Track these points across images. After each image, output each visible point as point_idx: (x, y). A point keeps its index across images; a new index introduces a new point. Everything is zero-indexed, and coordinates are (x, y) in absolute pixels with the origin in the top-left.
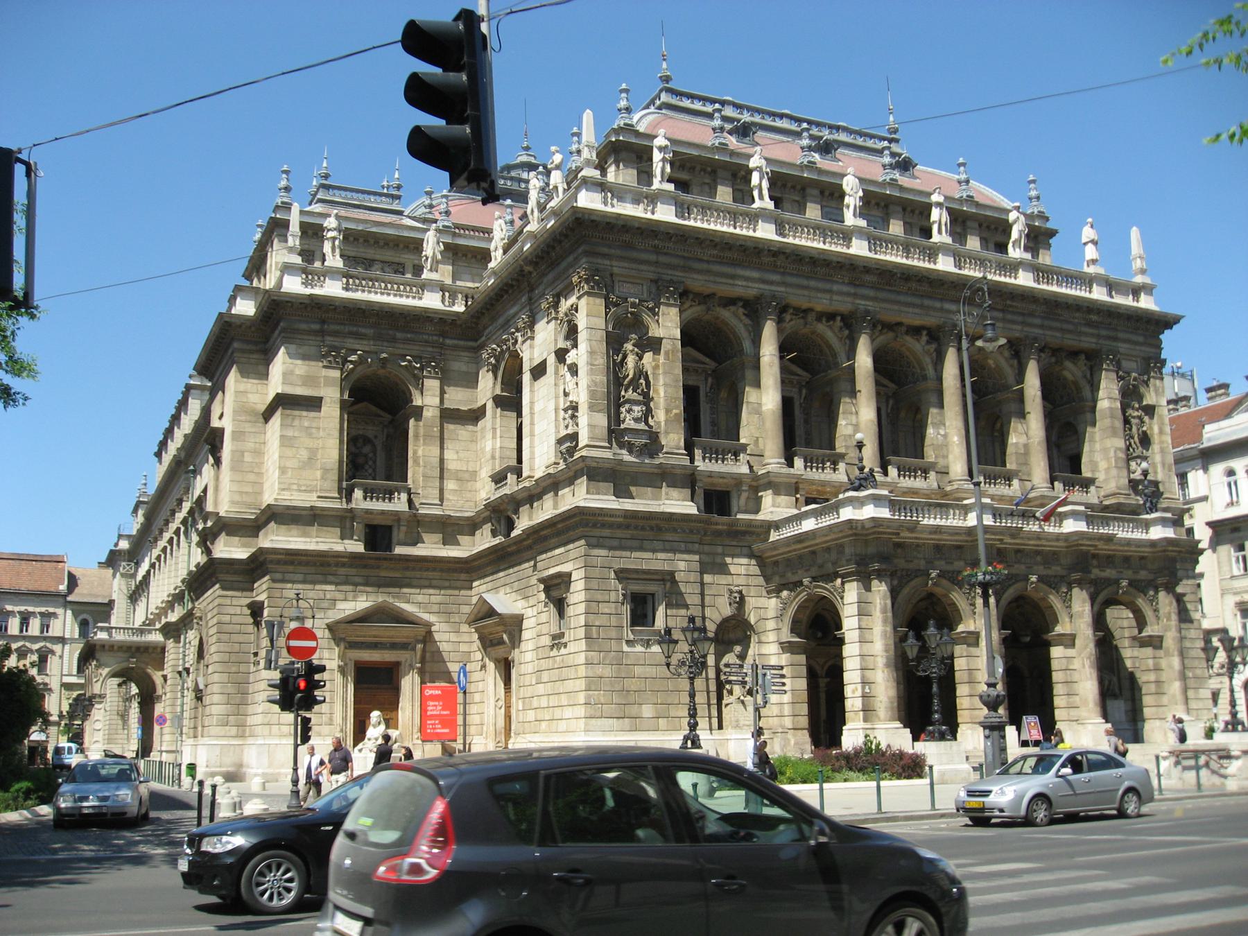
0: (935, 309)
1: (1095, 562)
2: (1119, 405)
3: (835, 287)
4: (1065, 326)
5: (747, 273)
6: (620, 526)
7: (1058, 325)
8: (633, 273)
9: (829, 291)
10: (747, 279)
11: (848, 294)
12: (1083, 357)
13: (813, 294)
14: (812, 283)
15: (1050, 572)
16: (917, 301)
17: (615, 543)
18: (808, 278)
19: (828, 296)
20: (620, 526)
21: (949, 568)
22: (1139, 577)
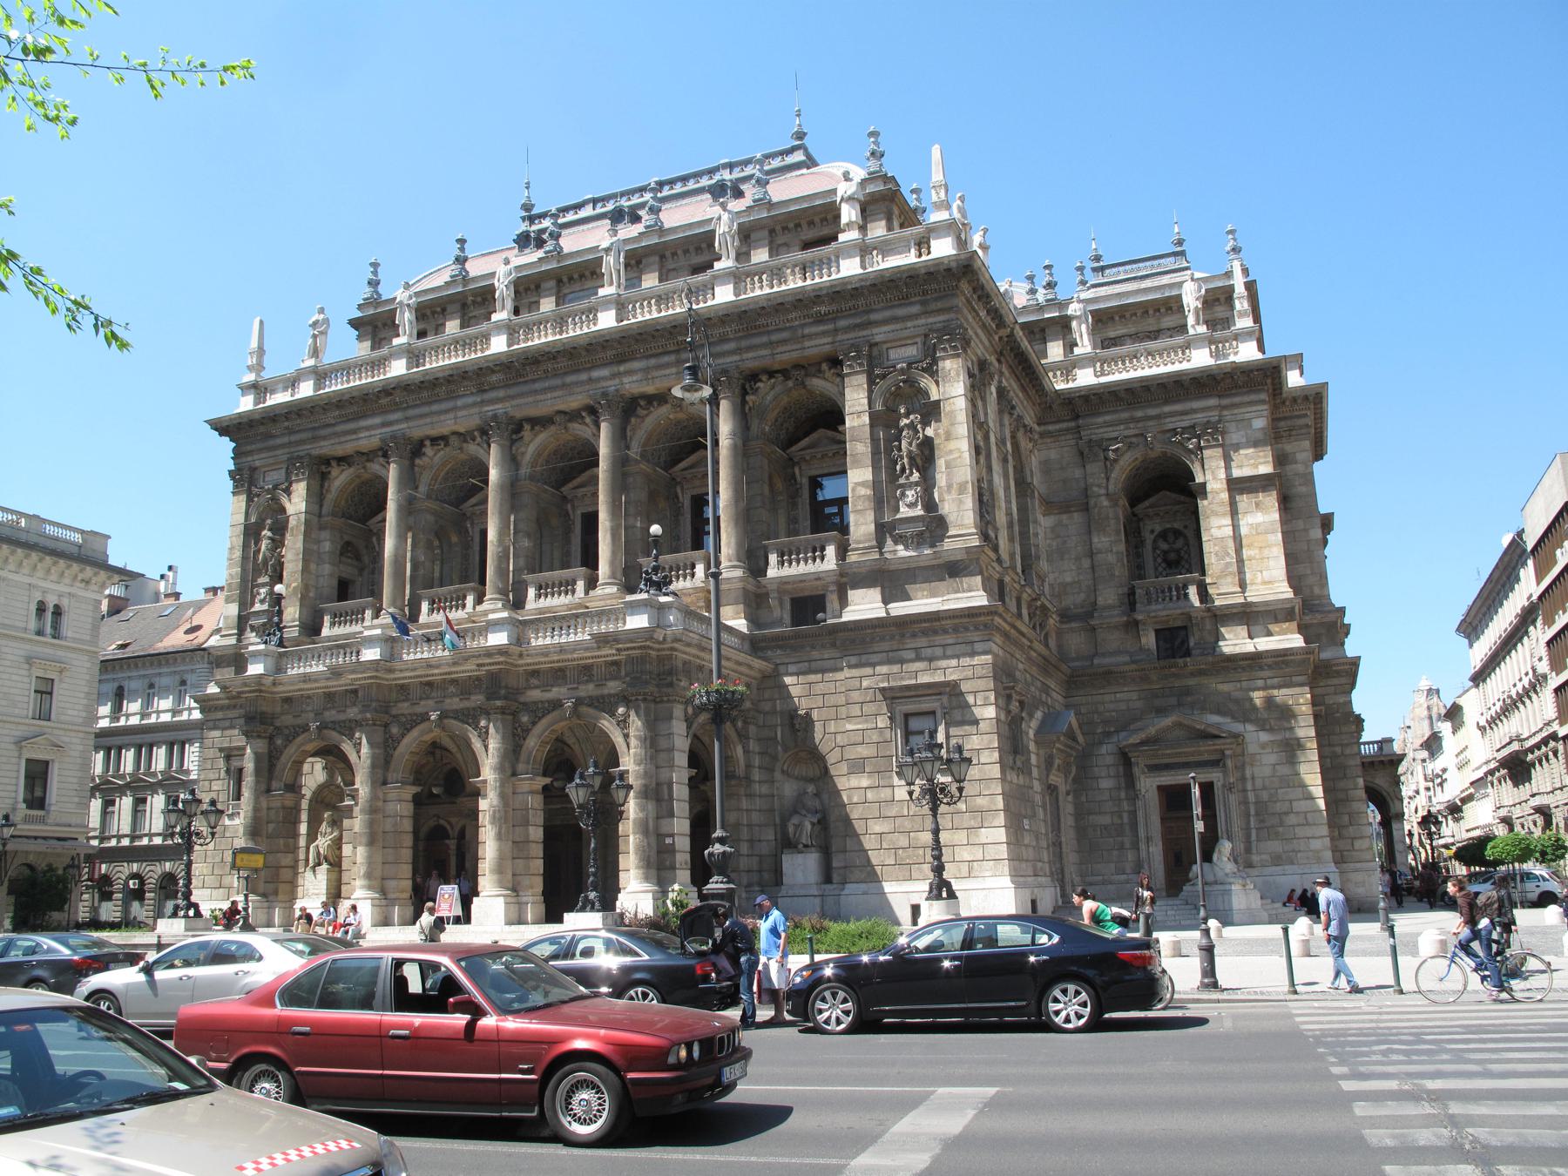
0: (582, 383)
1: (534, 681)
2: (866, 419)
3: (460, 403)
4: (774, 337)
5: (369, 422)
6: (228, 707)
7: (765, 339)
8: (271, 461)
9: (455, 409)
10: (367, 428)
11: (474, 404)
12: (824, 366)
13: (435, 419)
14: (435, 407)
15: (466, 704)
16: (558, 382)
17: (227, 723)
18: (430, 403)
19: (451, 415)
20: (228, 707)
21: (342, 717)
22: (606, 691)
